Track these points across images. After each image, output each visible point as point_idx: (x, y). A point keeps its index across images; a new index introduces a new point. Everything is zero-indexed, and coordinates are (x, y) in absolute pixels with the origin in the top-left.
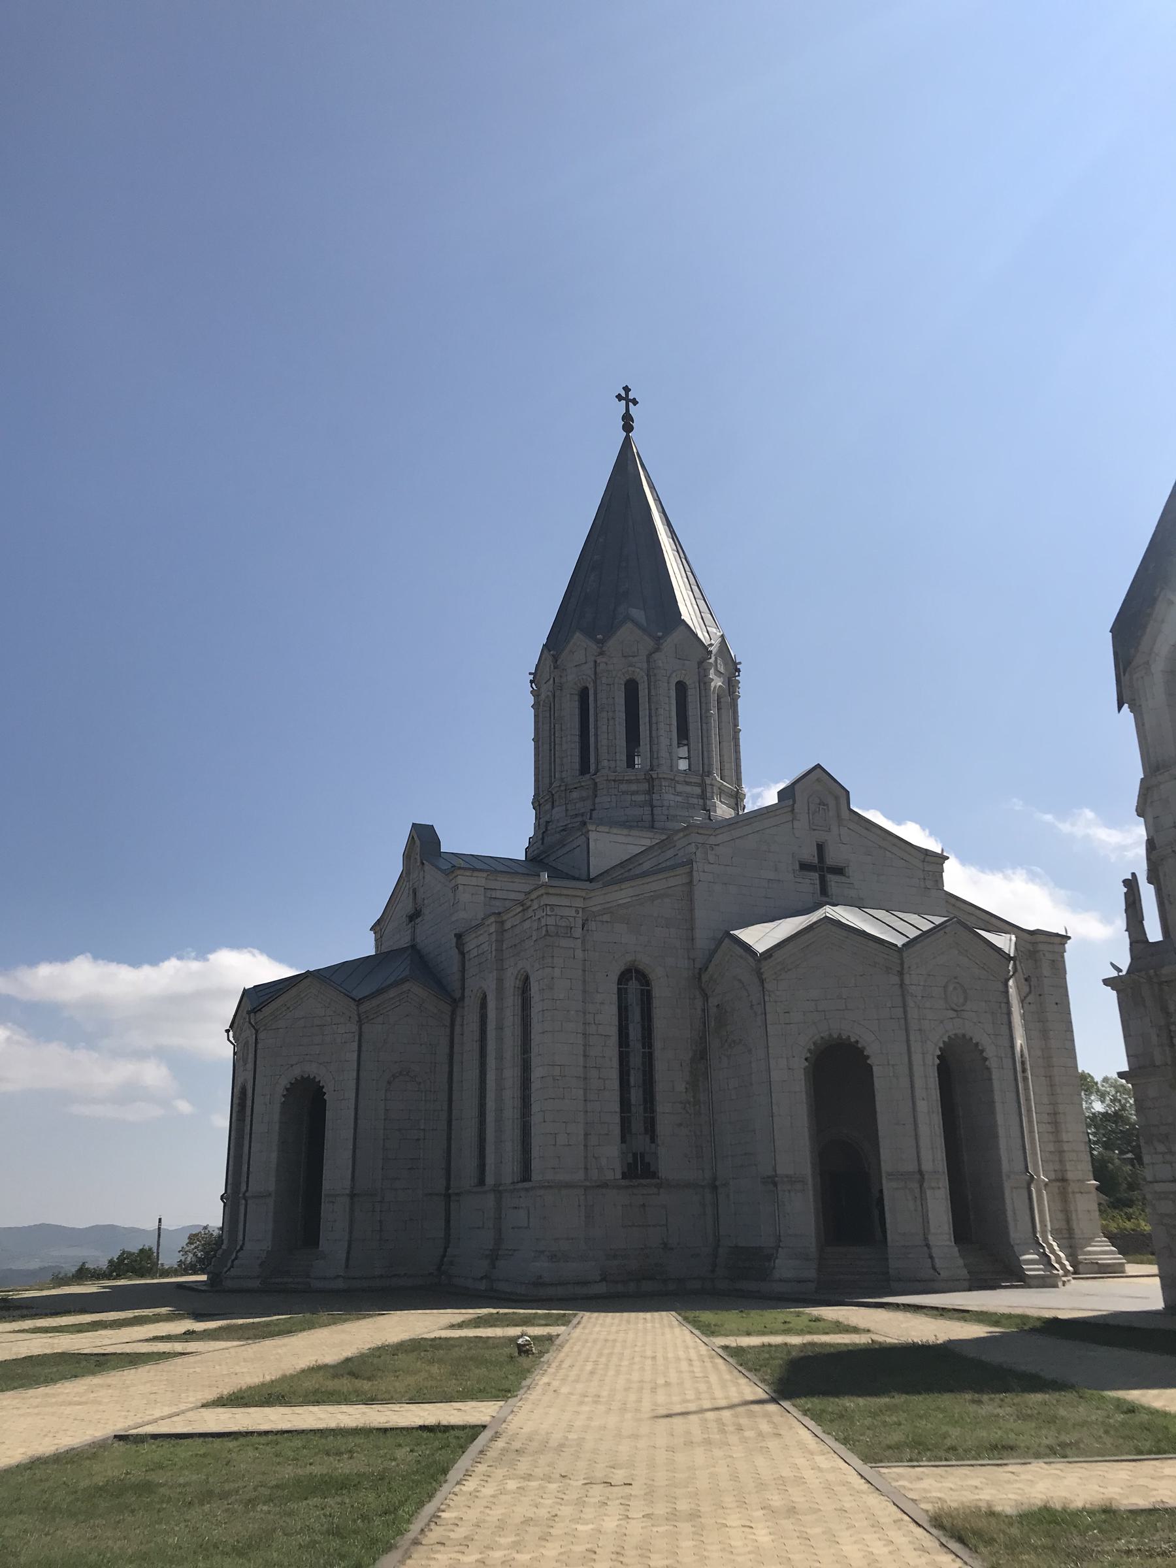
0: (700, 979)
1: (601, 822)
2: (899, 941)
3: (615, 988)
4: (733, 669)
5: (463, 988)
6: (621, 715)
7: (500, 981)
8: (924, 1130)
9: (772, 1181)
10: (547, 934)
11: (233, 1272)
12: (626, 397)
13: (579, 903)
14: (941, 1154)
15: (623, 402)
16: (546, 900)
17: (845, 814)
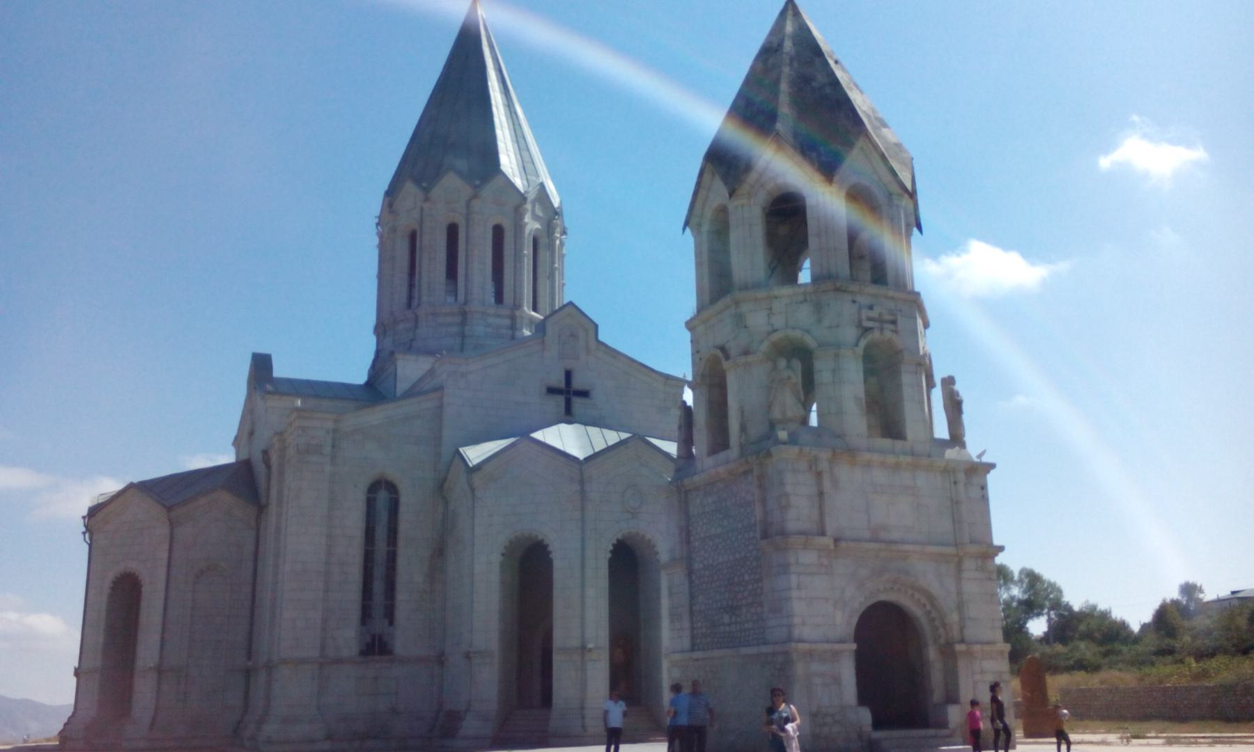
4: (552, 216)
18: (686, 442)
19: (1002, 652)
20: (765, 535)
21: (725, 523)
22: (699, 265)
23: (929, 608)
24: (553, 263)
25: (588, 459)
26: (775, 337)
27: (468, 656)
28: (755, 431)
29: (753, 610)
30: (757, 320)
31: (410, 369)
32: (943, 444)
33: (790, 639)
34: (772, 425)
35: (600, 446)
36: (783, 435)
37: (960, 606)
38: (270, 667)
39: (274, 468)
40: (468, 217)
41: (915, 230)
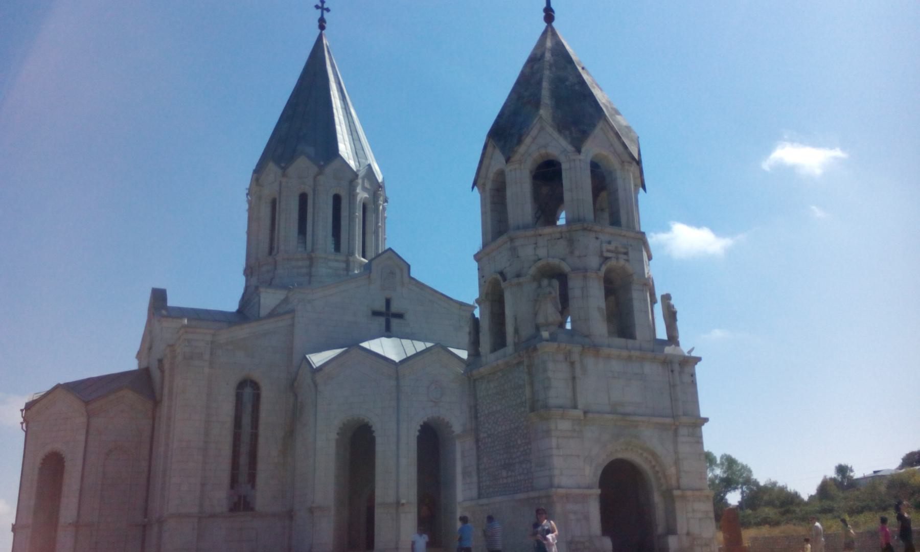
4: (377, 189)
12: (322, 7)
15: (320, 11)
18: (474, 346)
19: (708, 497)
20: (533, 409)
22: (484, 213)
23: (653, 463)
24: (377, 223)
25: (402, 362)
26: (540, 264)
27: (311, 510)
28: (526, 332)
29: (524, 466)
30: (527, 252)
31: (269, 299)
32: (662, 343)
33: (551, 486)
34: (538, 328)
35: (411, 352)
36: (545, 334)
37: (677, 462)
38: (161, 521)
39: (167, 373)
41: (641, 190)
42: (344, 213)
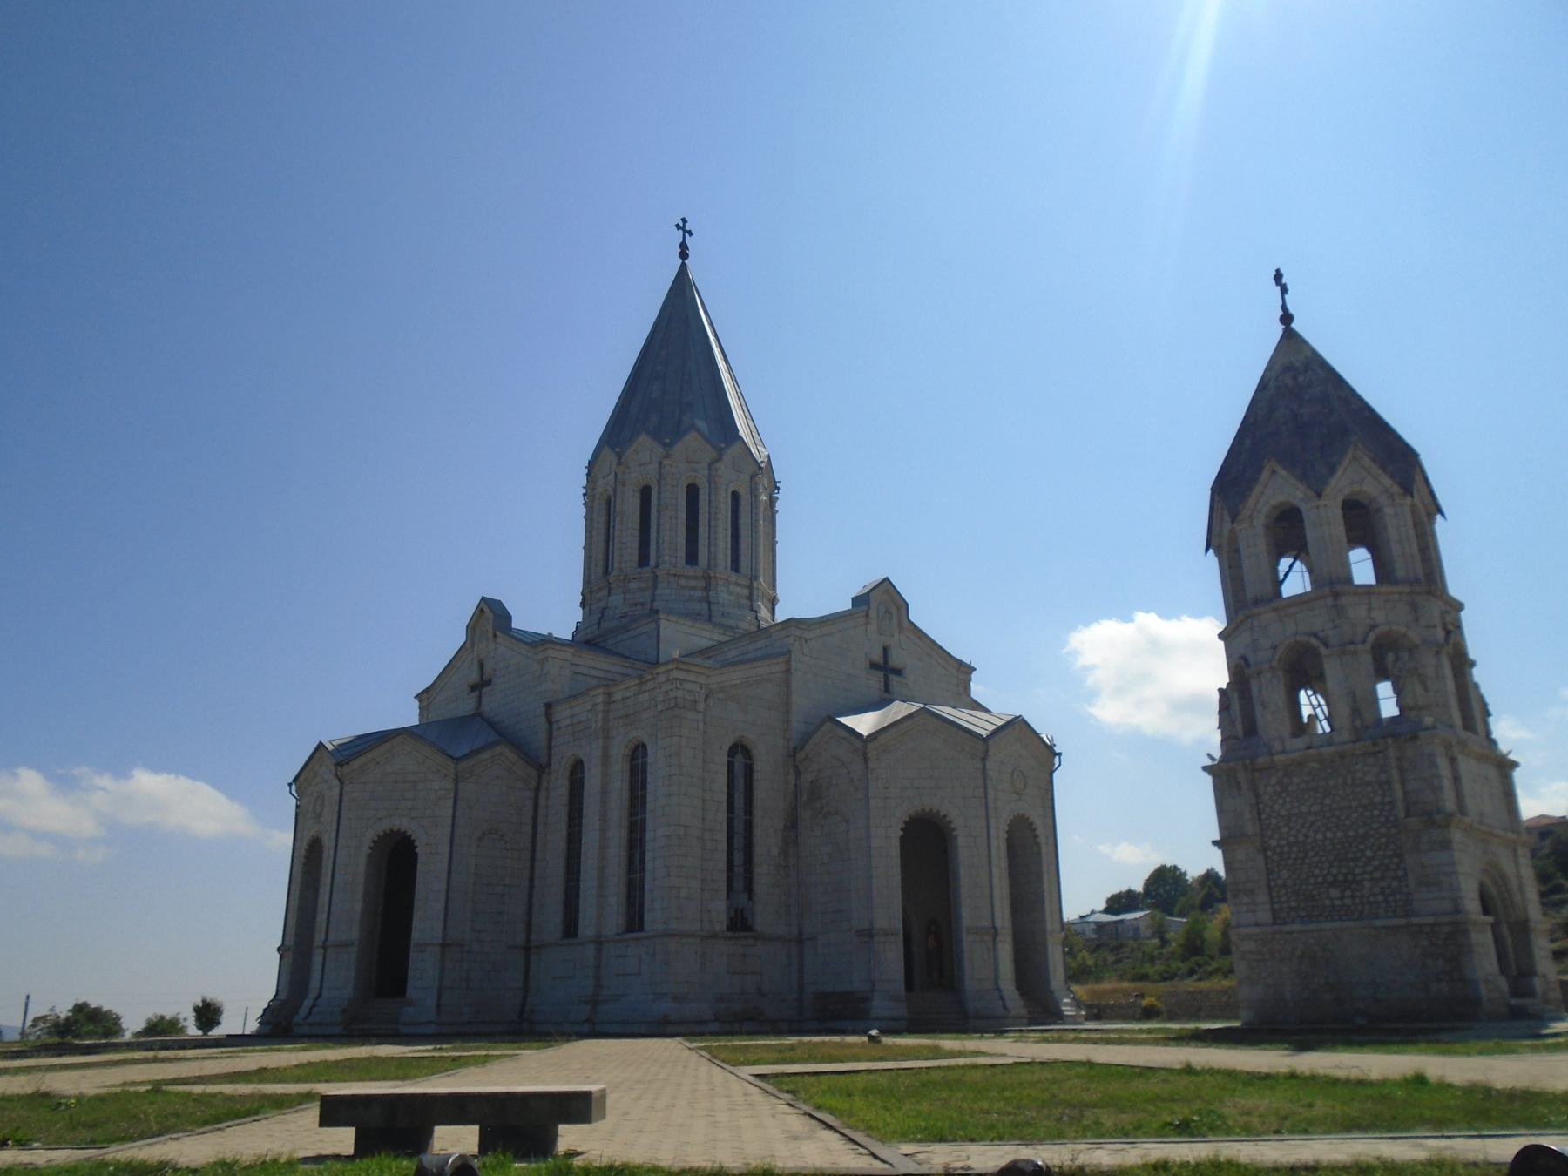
0: (795, 755)
1: (670, 613)
2: (984, 733)
3: (725, 759)
4: (775, 486)
5: (550, 755)
6: (682, 515)
7: (606, 748)
8: (996, 892)
9: (868, 934)
10: (676, 705)
11: (311, 1019)
13: (702, 680)
14: (1007, 913)
16: (675, 674)
17: (905, 623)
21: (1327, 801)
26: (1378, 631)
29: (1384, 884)
37: (1521, 887)
40: (711, 480)
42: (744, 519)
